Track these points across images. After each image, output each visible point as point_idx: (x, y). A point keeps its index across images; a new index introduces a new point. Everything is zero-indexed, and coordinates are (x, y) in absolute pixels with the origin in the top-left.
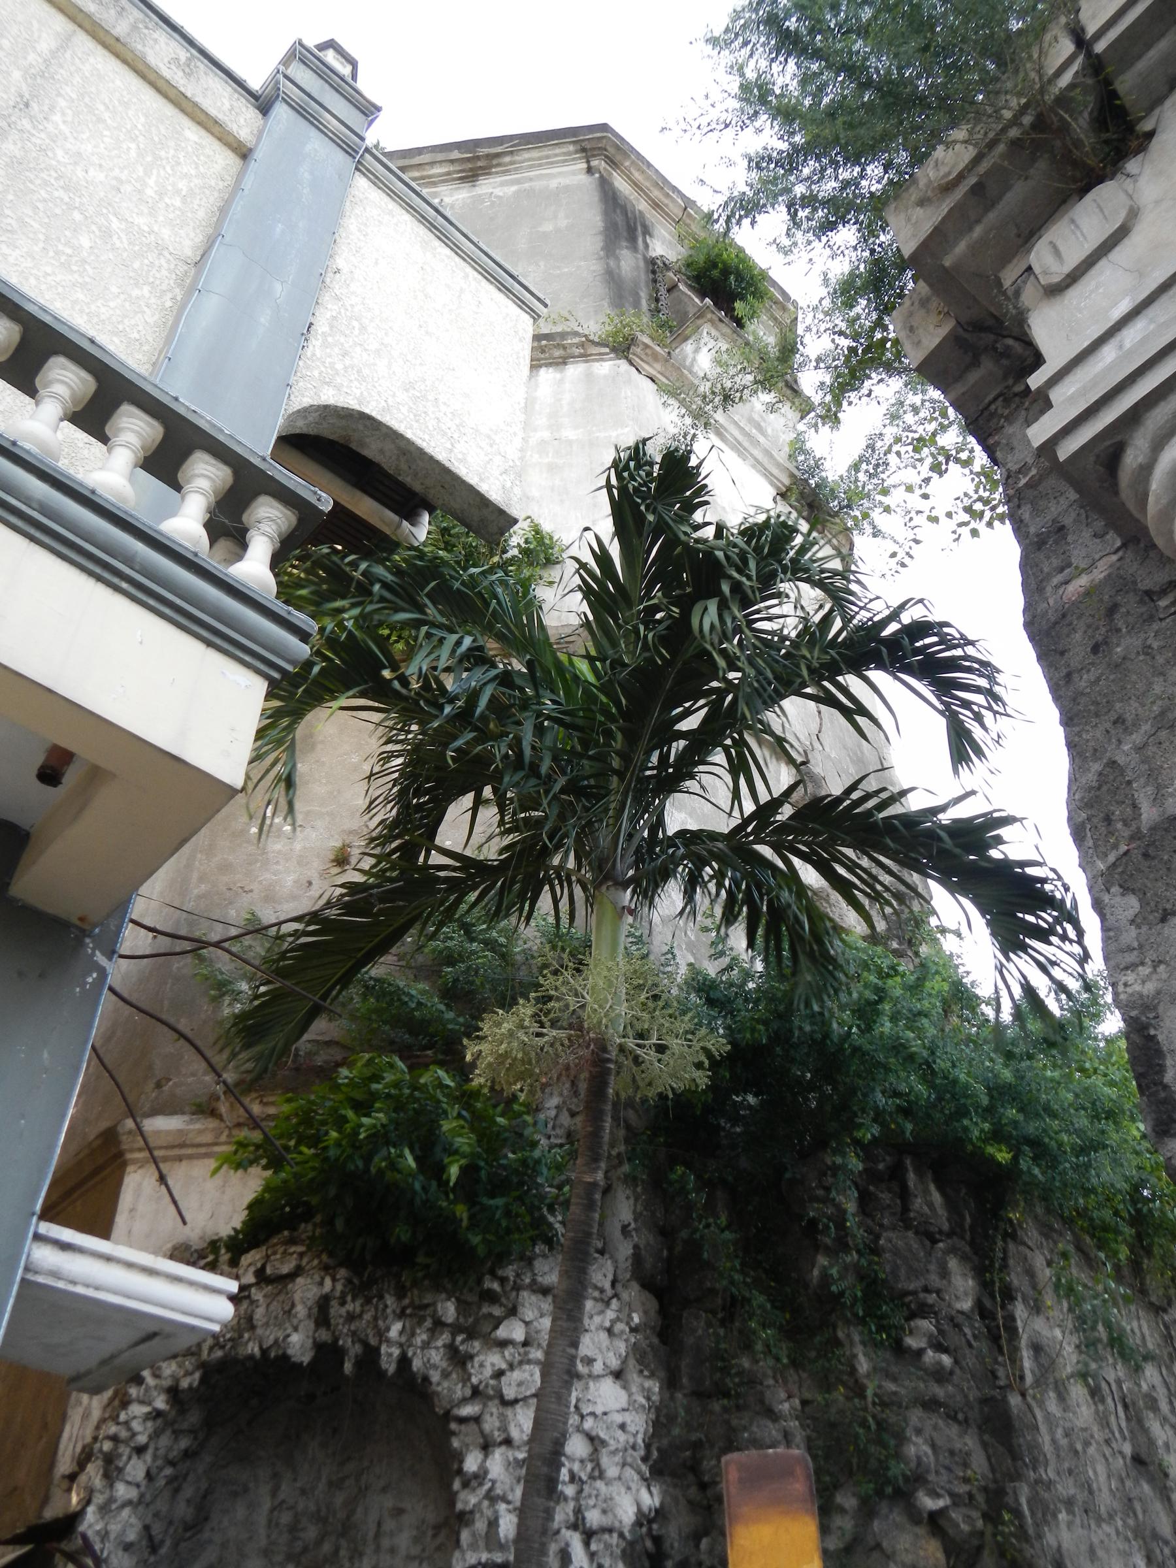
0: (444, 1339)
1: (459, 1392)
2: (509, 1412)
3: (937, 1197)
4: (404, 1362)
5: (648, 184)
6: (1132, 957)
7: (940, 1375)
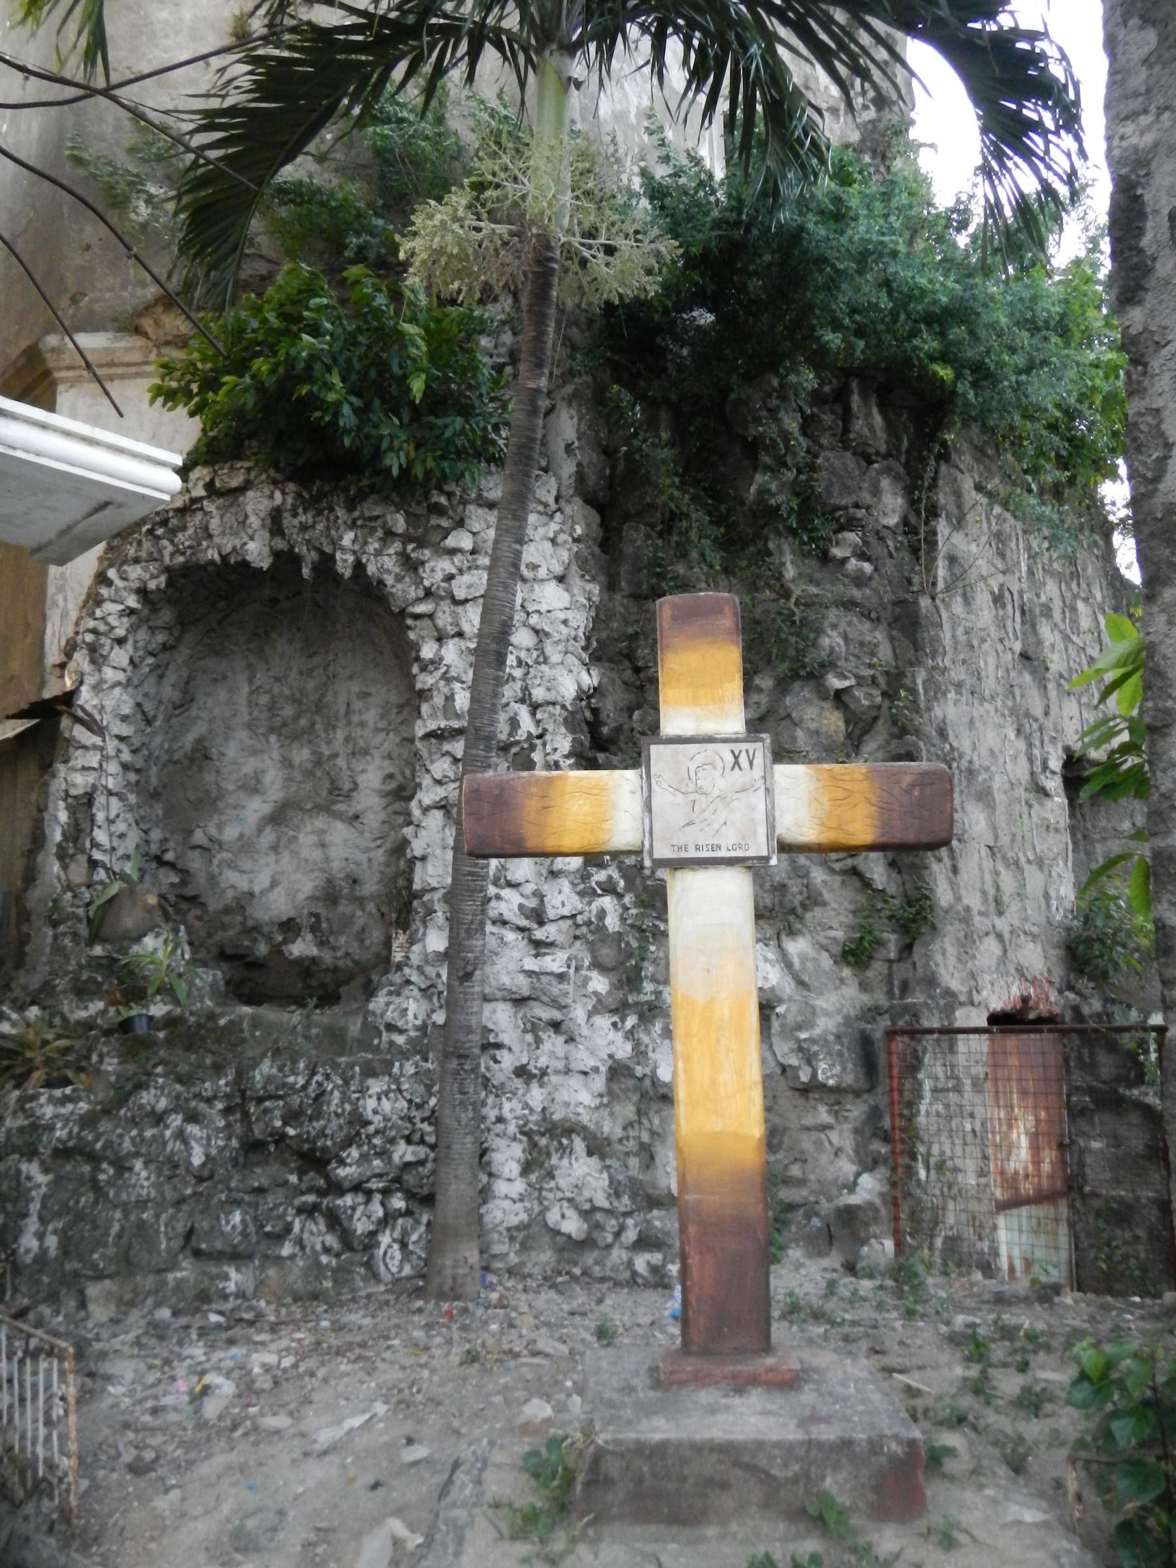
0: (396, 546)
1: (413, 593)
2: (460, 609)
3: (878, 420)
4: (359, 567)
6: (1135, 105)
7: (860, 580)
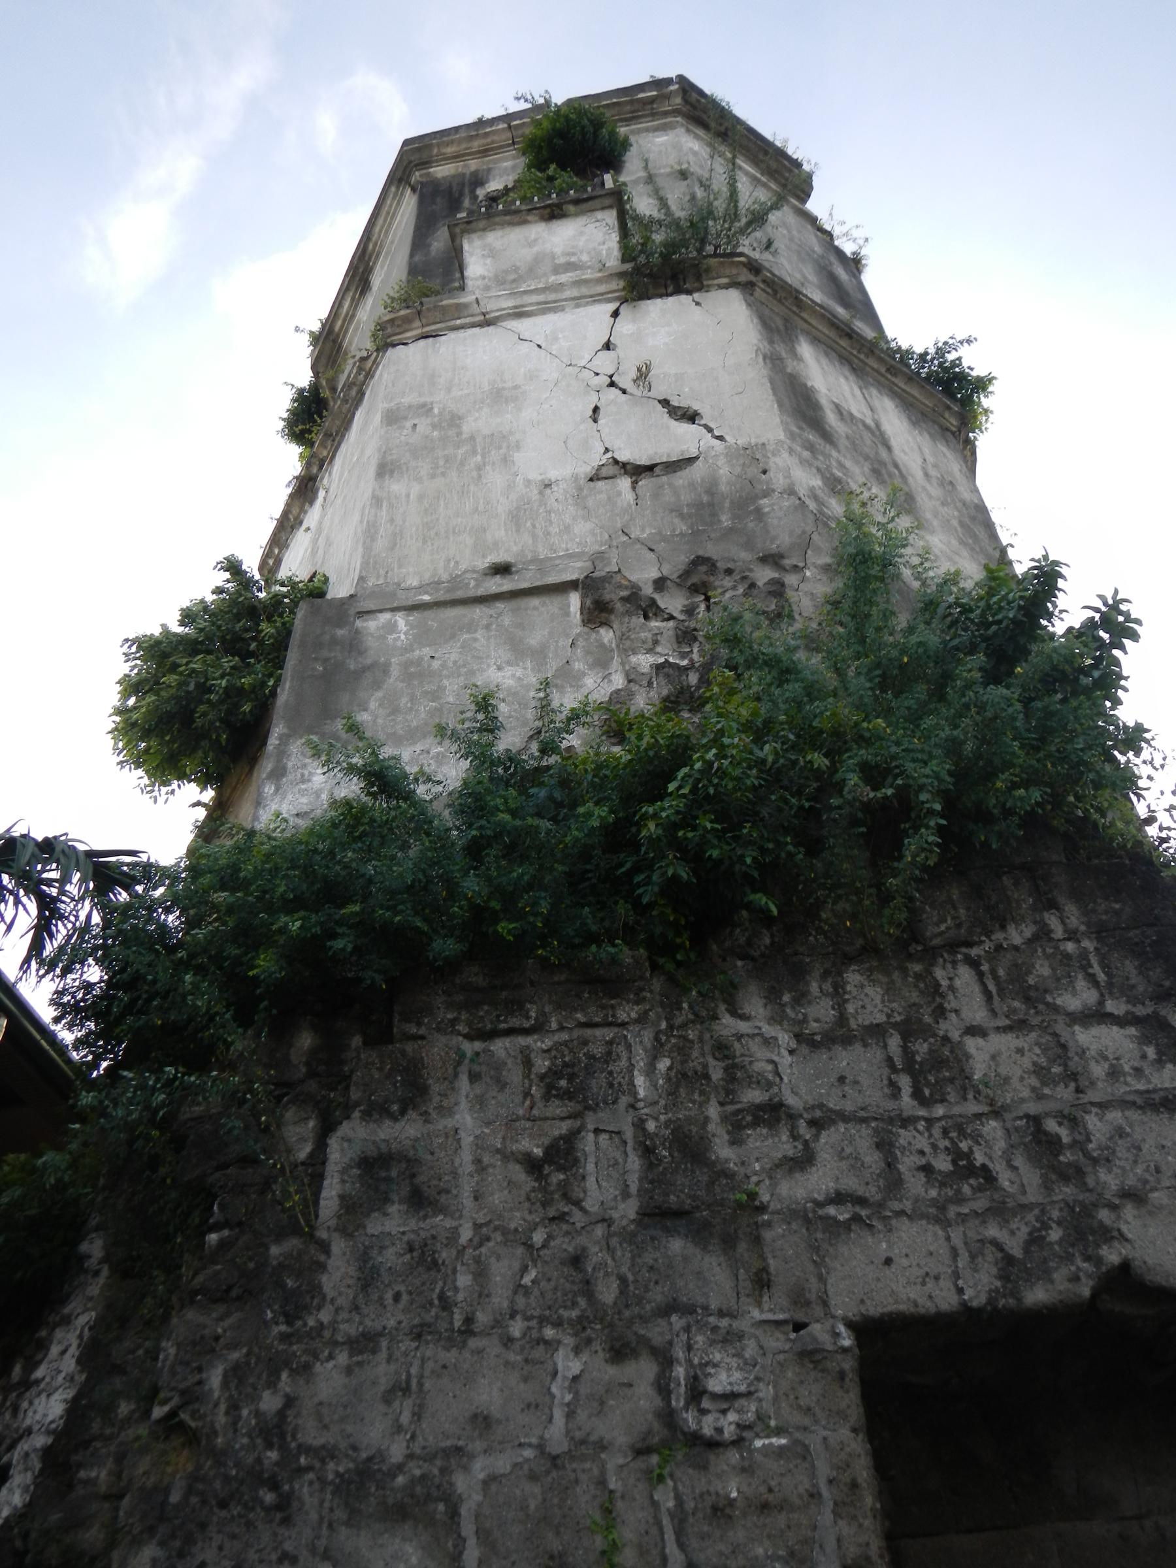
5: (464, 146)
